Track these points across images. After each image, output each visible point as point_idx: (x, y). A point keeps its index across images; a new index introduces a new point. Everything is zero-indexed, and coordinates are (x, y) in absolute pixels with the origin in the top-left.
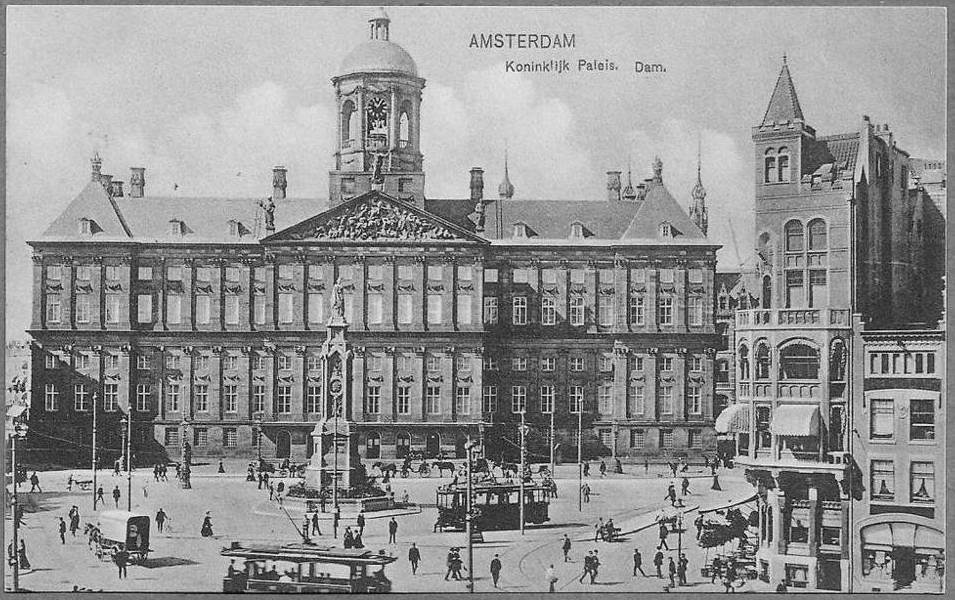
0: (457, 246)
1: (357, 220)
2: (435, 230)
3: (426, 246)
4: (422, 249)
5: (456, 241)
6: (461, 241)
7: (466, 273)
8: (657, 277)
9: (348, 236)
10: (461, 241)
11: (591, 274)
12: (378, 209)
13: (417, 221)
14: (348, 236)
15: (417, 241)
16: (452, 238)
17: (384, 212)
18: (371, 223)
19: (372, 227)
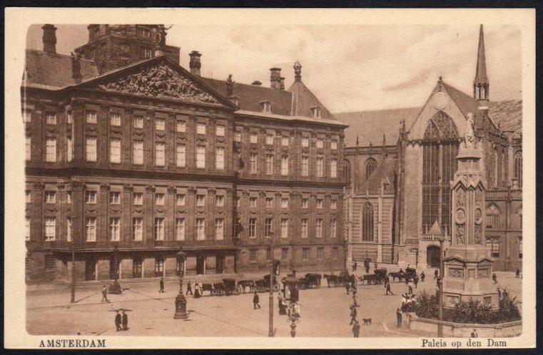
0: (217, 109)
1: (149, 79)
2: (202, 95)
3: (197, 107)
4: (193, 109)
5: (216, 104)
6: (220, 105)
7: (220, 131)
8: (313, 144)
9: (143, 92)
10: (220, 105)
11: (277, 139)
12: (165, 72)
13: (192, 86)
14: (143, 92)
15: (192, 100)
16: (213, 102)
17: (167, 76)
18: (160, 82)
19: (160, 86)
